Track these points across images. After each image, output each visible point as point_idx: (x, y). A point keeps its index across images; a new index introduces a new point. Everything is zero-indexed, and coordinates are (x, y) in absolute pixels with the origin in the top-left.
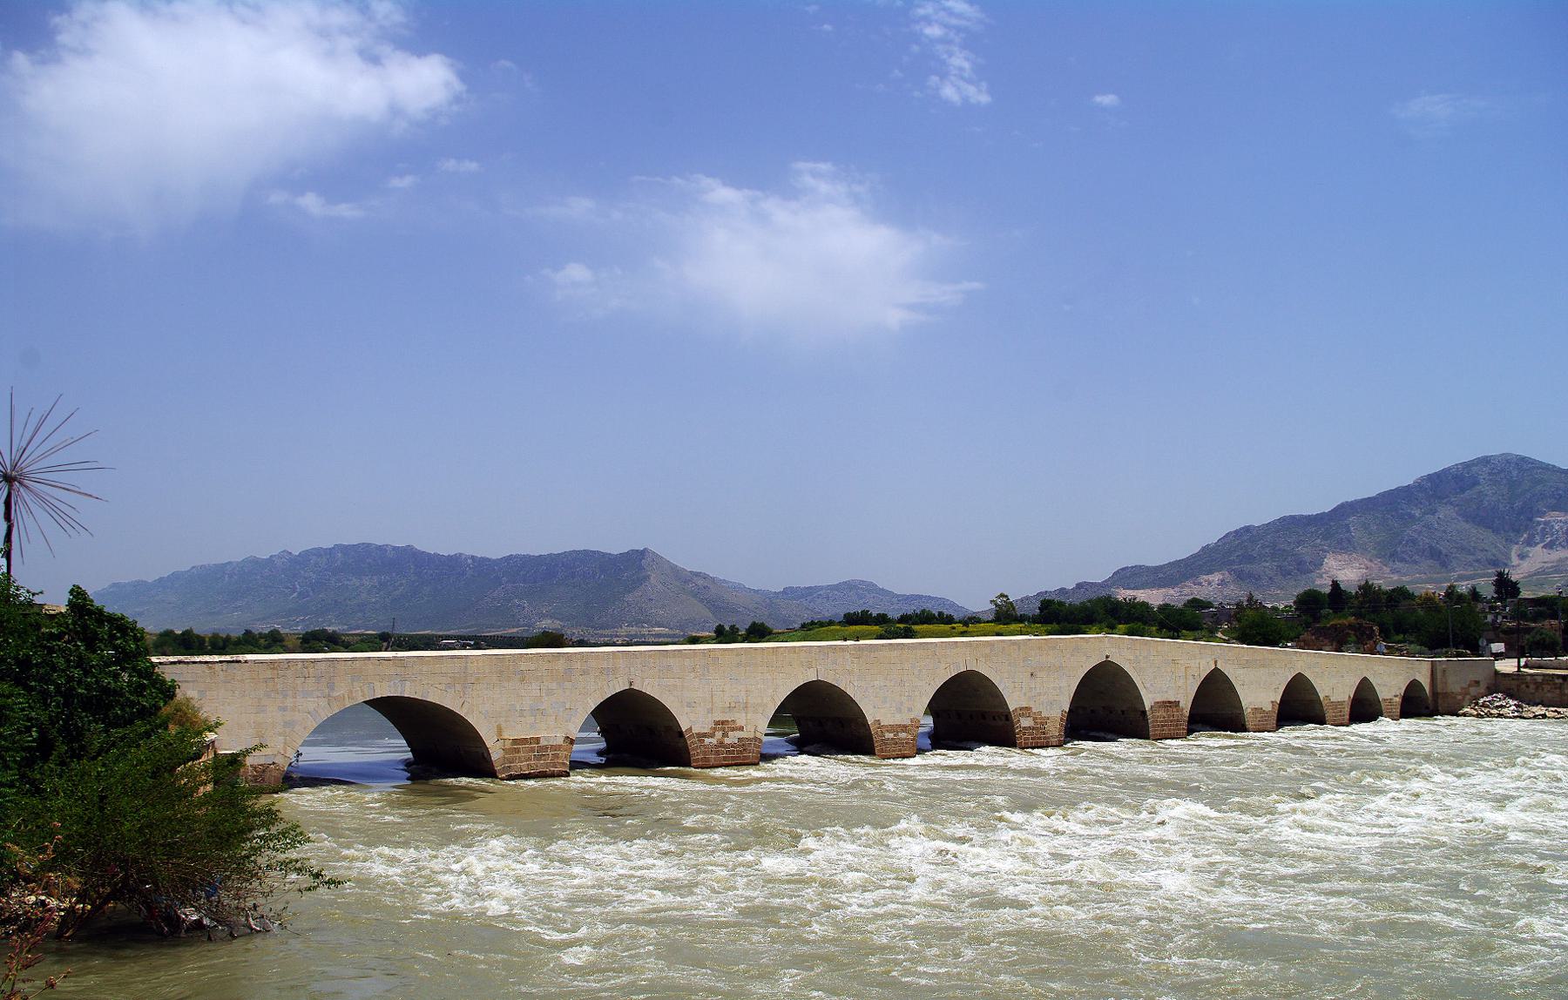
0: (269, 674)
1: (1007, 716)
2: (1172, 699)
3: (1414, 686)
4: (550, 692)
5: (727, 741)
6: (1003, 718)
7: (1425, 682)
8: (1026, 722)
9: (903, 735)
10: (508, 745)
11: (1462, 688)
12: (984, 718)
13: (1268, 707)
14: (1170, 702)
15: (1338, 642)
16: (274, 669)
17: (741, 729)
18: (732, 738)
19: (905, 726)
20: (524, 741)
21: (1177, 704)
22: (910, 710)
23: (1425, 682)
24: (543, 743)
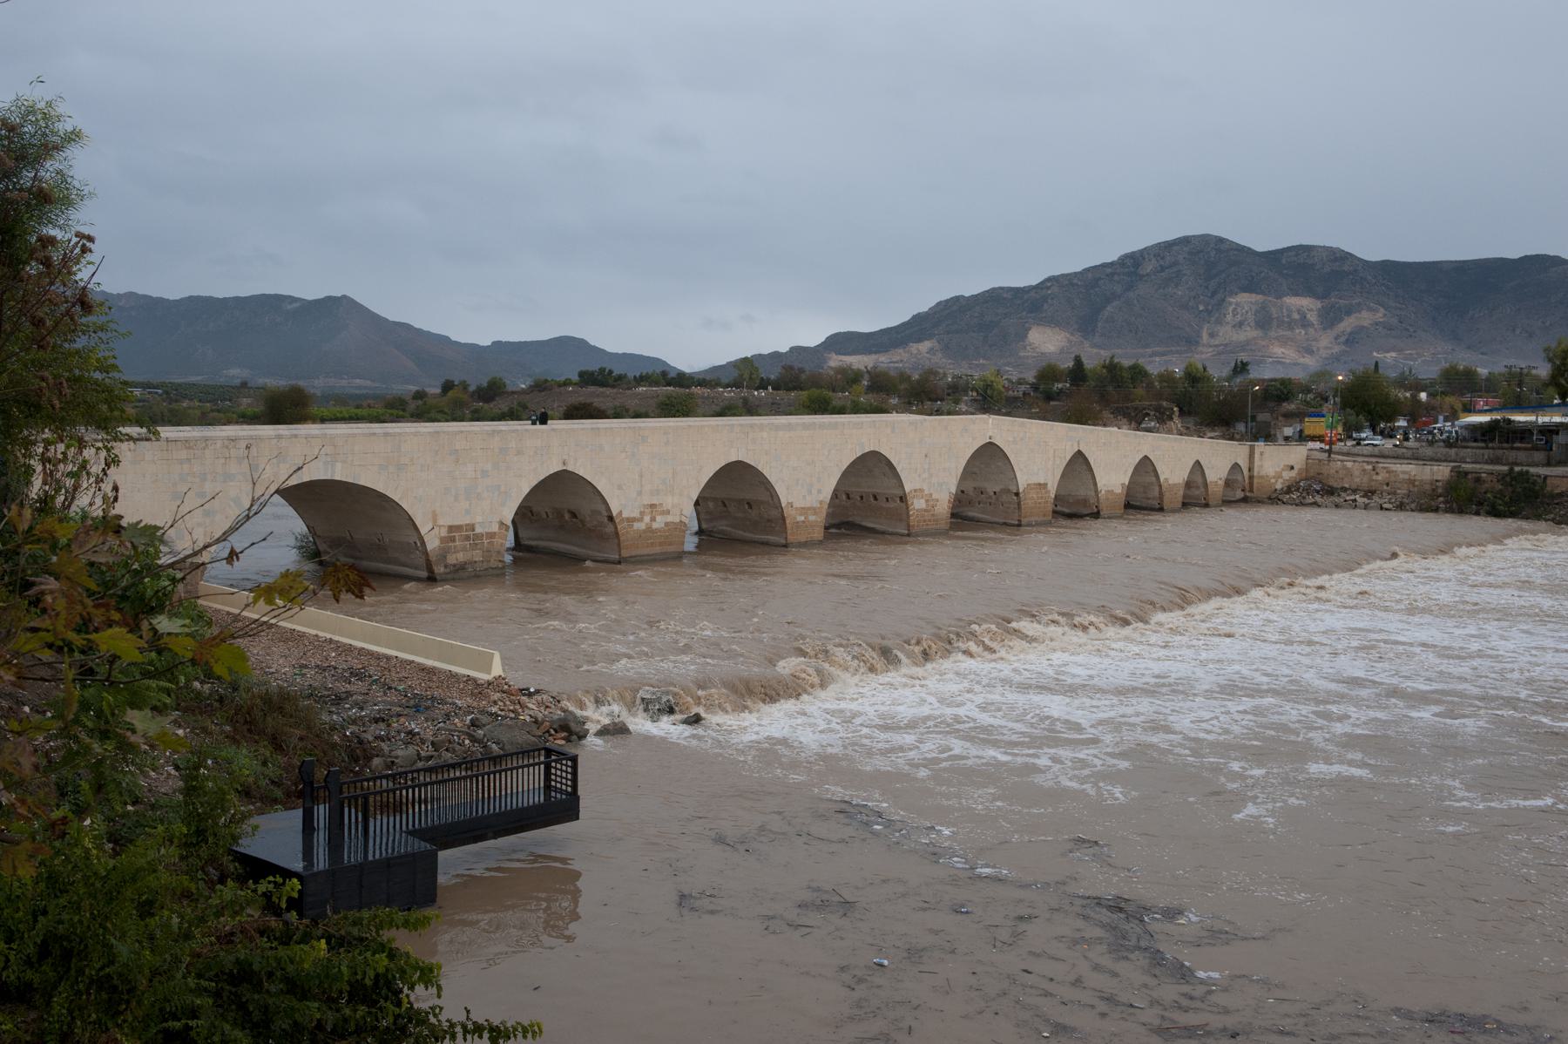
0: (183, 454)
1: (903, 499)
2: (1042, 482)
3: (1236, 467)
4: (485, 473)
5: (655, 526)
6: (898, 500)
7: (1244, 465)
8: (918, 504)
9: (812, 518)
10: (444, 533)
11: (1276, 472)
12: (875, 498)
13: (1119, 490)
14: (1040, 484)
15: (1136, 422)
16: (189, 448)
17: (668, 512)
18: (659, 523)
19: (814, 509)
20: (458, 528)
21: (1046, 485)
22: (819, 491)
23: (1244, 465)
24: (478, 530)
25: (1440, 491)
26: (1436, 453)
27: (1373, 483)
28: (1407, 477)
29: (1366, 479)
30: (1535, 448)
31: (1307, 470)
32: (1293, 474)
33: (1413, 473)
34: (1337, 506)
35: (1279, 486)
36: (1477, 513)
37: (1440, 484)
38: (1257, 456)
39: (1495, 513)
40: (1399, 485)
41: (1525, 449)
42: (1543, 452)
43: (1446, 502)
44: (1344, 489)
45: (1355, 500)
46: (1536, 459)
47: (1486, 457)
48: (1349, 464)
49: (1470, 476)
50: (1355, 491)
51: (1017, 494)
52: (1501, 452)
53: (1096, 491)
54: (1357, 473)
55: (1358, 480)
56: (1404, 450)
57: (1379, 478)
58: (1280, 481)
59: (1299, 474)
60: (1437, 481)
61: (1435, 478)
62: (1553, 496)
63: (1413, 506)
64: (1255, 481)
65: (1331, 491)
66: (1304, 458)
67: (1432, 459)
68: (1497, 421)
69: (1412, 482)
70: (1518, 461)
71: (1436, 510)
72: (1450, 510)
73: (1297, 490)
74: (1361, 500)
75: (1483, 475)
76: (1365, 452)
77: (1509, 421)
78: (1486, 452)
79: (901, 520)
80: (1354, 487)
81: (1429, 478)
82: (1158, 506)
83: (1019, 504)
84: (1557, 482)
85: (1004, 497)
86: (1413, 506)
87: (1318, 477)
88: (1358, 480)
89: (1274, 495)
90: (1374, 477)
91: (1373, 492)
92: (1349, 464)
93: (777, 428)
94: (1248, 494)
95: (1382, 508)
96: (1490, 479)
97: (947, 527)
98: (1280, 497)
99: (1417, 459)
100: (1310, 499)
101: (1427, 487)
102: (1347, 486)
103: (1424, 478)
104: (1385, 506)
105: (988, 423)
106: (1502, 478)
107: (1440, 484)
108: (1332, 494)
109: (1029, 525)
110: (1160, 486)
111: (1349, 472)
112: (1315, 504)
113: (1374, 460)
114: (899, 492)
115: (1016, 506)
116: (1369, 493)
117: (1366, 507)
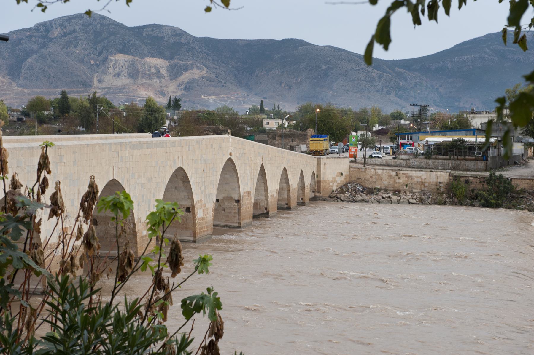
11: (333, 178)
14: (248, 192)
25: (442, 189)
26: (421, 163)
27: (396, 185)
28: (419, 180)
29: (391, 182)
30: (476, 160)
31: (350, 176)
32: (342, 179)
33: (423, 178)
34: (379, 202)
35: (334, 188)
36: (472, 205)
37: (442, 185)
38: (322, 166)
39: (487, 204)
40: (414, 186)
41: (471, 160)
42: (483, 162)
43: (448, 198)
44: (379, 190)
45: (389, 197)
46: (479, 167)
47: (450, 165)
48: (380, 172)
49: (462, 179)
50: (386, 190)
51: (238, 201)
52: (459, 162)
53: (267, 196)
54: (385, 178)
55: (386, 183)
56: (401, 161)
57: (401, 181)
58: (335, 184)
59: (345, 179)
60: (440, 183)
61: (439, 181)
62: (519, 193)
63: (429, 200)
64: (322, 184)
65: (371, 191)
66: (348, 168)
67: (418, 167)
68: (455, 141)
69: (423, 183)
70: (469, 168)
71: (445, 203)
72: (453, 204)
73: (348, 190)
74: (394, 197)
75: (471, 178)
76: (377, 163)
77: (463, 141)
78: (450, 162)
79: (186, 229)
80: (383, 187)
81: (435, 180)
82: (286, 206)
83: (239, 209)
84: (518, 182)
85: (226, 203)
86: (429, 200)
87: (358, 181)
88: (386, 183)
89: (333, 195)
90: (398, 181)
91: (400, 191)
92: (380, 172)
93: (133, 146)
94: (317, 194)
95: (409, 203)
96: (474, 181)
97: (210, 232)
98: (338, 196)
99: (409, 167)
100: (359, 198)
101: (434, 187)
102: (379, 187)
103: (431, 181)
104: (411, 201)
105: (228, 141)
106: (484, 180)
107: (442, 185)
108: (372, 193)
109: (244, 226)
110: (289, 190)
111: (380, 178)
112: (364, 200)
113: (397, 168)
114: (188, 204)
115: (237, 211)
116: (397, 192)
117: (399, 202)
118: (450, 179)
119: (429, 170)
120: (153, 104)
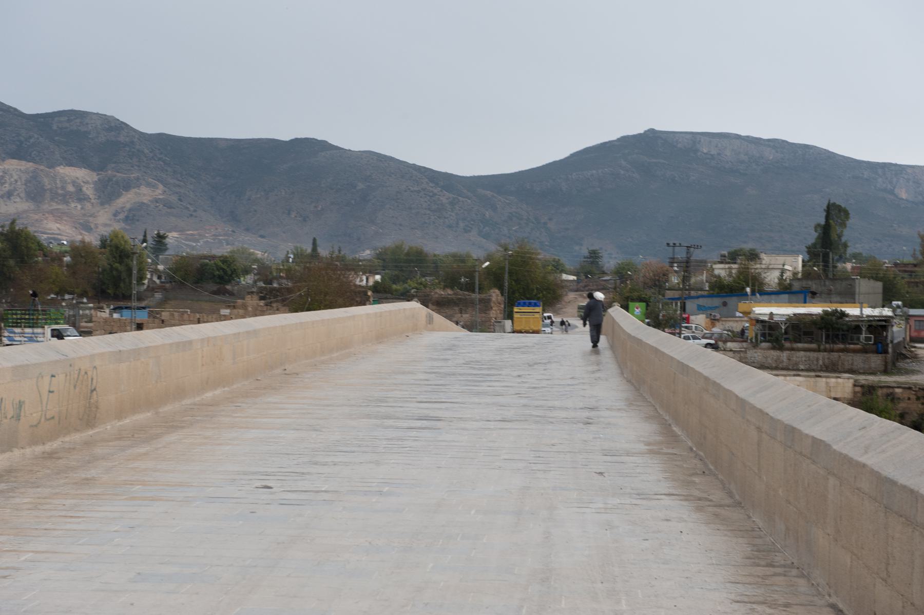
26: (766, 358)
30: (865, 351)
41: (855, 351)
42: (880, 355)
46: (873, 365)
47: (821, 362)
49: (880, 392)
52: (836, 355)
70: (855, 368)
75: (898, 391)
77: (843, 314)
78: (821, 355)
96: (906, 396)
118: (855, 393)
119: (813, 374)
120: (123, 243)
